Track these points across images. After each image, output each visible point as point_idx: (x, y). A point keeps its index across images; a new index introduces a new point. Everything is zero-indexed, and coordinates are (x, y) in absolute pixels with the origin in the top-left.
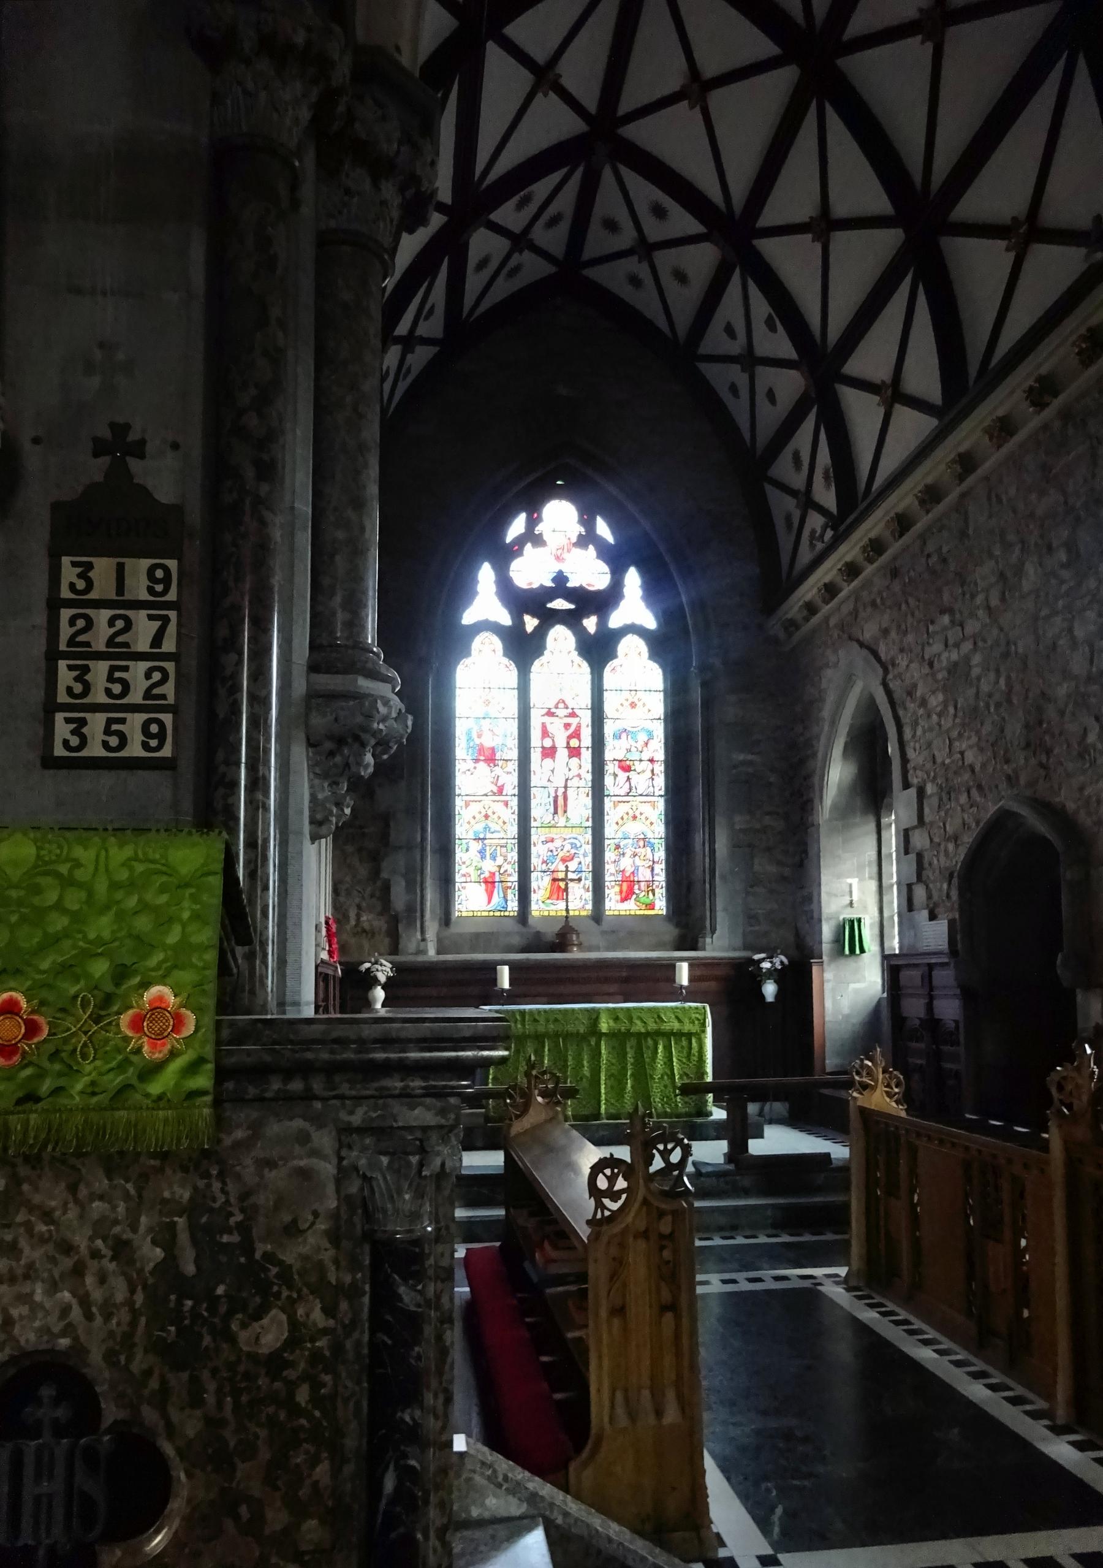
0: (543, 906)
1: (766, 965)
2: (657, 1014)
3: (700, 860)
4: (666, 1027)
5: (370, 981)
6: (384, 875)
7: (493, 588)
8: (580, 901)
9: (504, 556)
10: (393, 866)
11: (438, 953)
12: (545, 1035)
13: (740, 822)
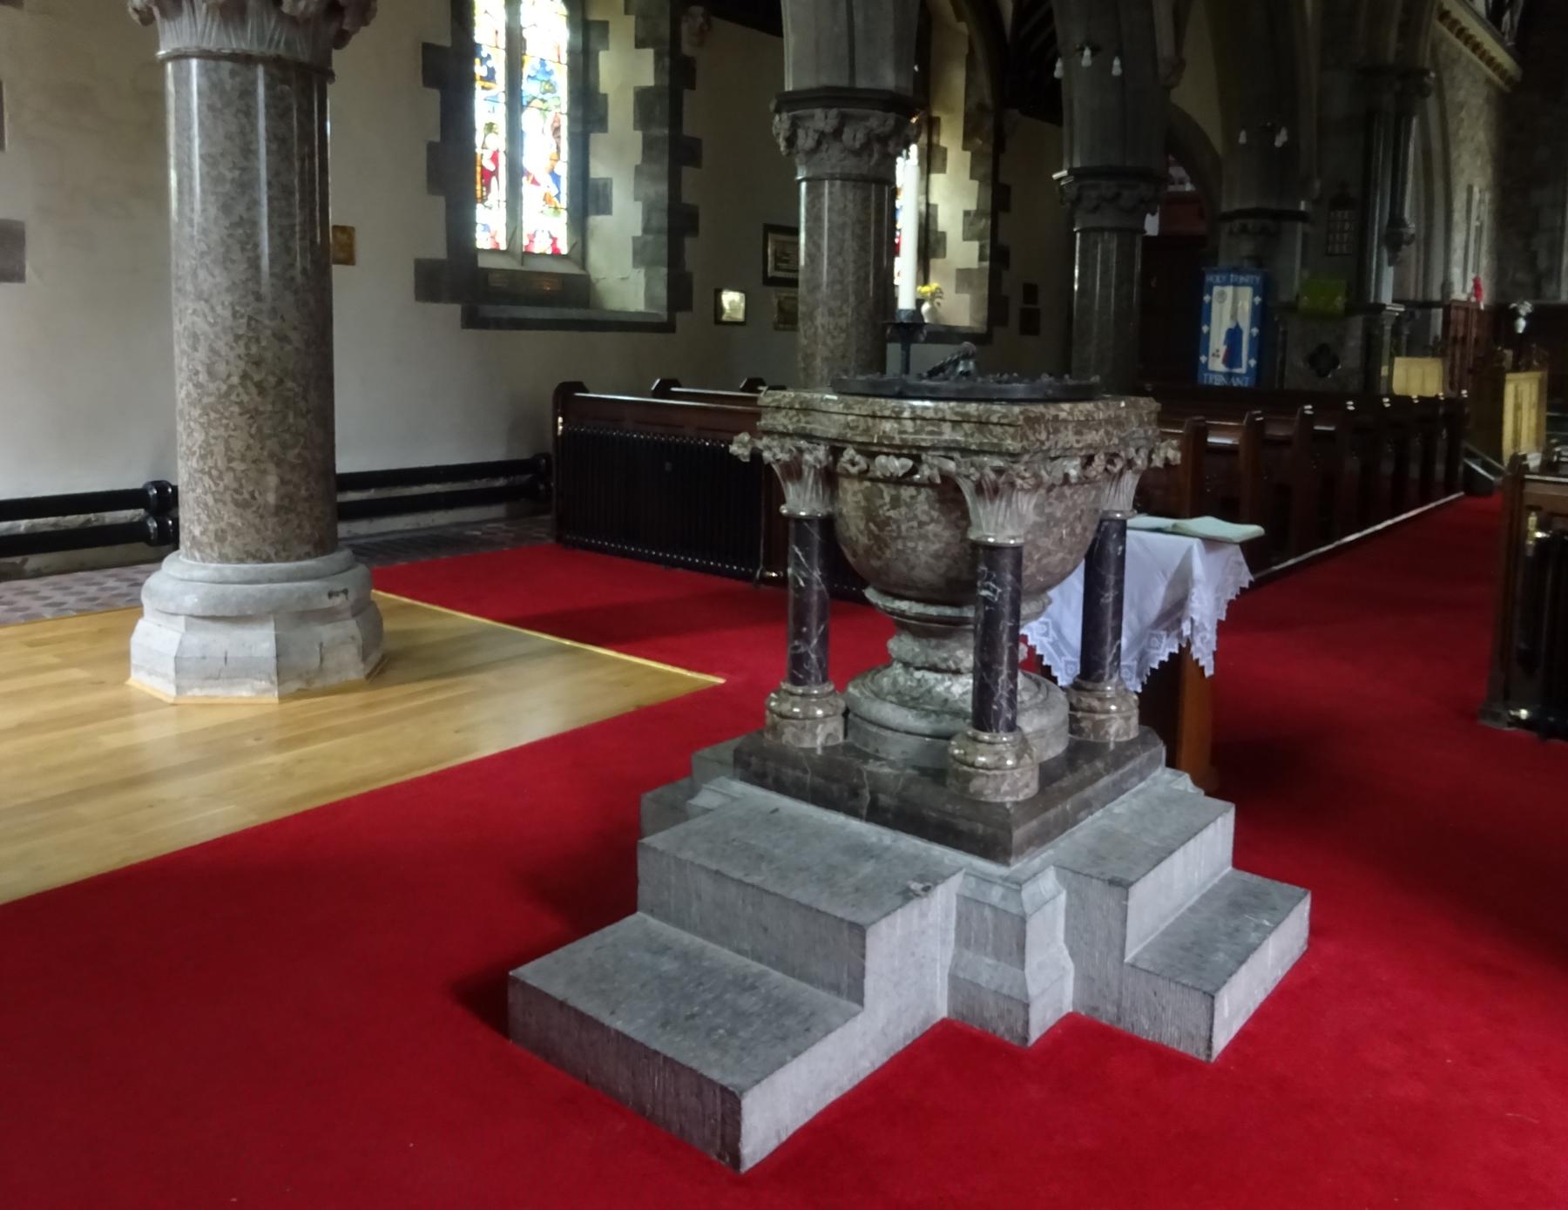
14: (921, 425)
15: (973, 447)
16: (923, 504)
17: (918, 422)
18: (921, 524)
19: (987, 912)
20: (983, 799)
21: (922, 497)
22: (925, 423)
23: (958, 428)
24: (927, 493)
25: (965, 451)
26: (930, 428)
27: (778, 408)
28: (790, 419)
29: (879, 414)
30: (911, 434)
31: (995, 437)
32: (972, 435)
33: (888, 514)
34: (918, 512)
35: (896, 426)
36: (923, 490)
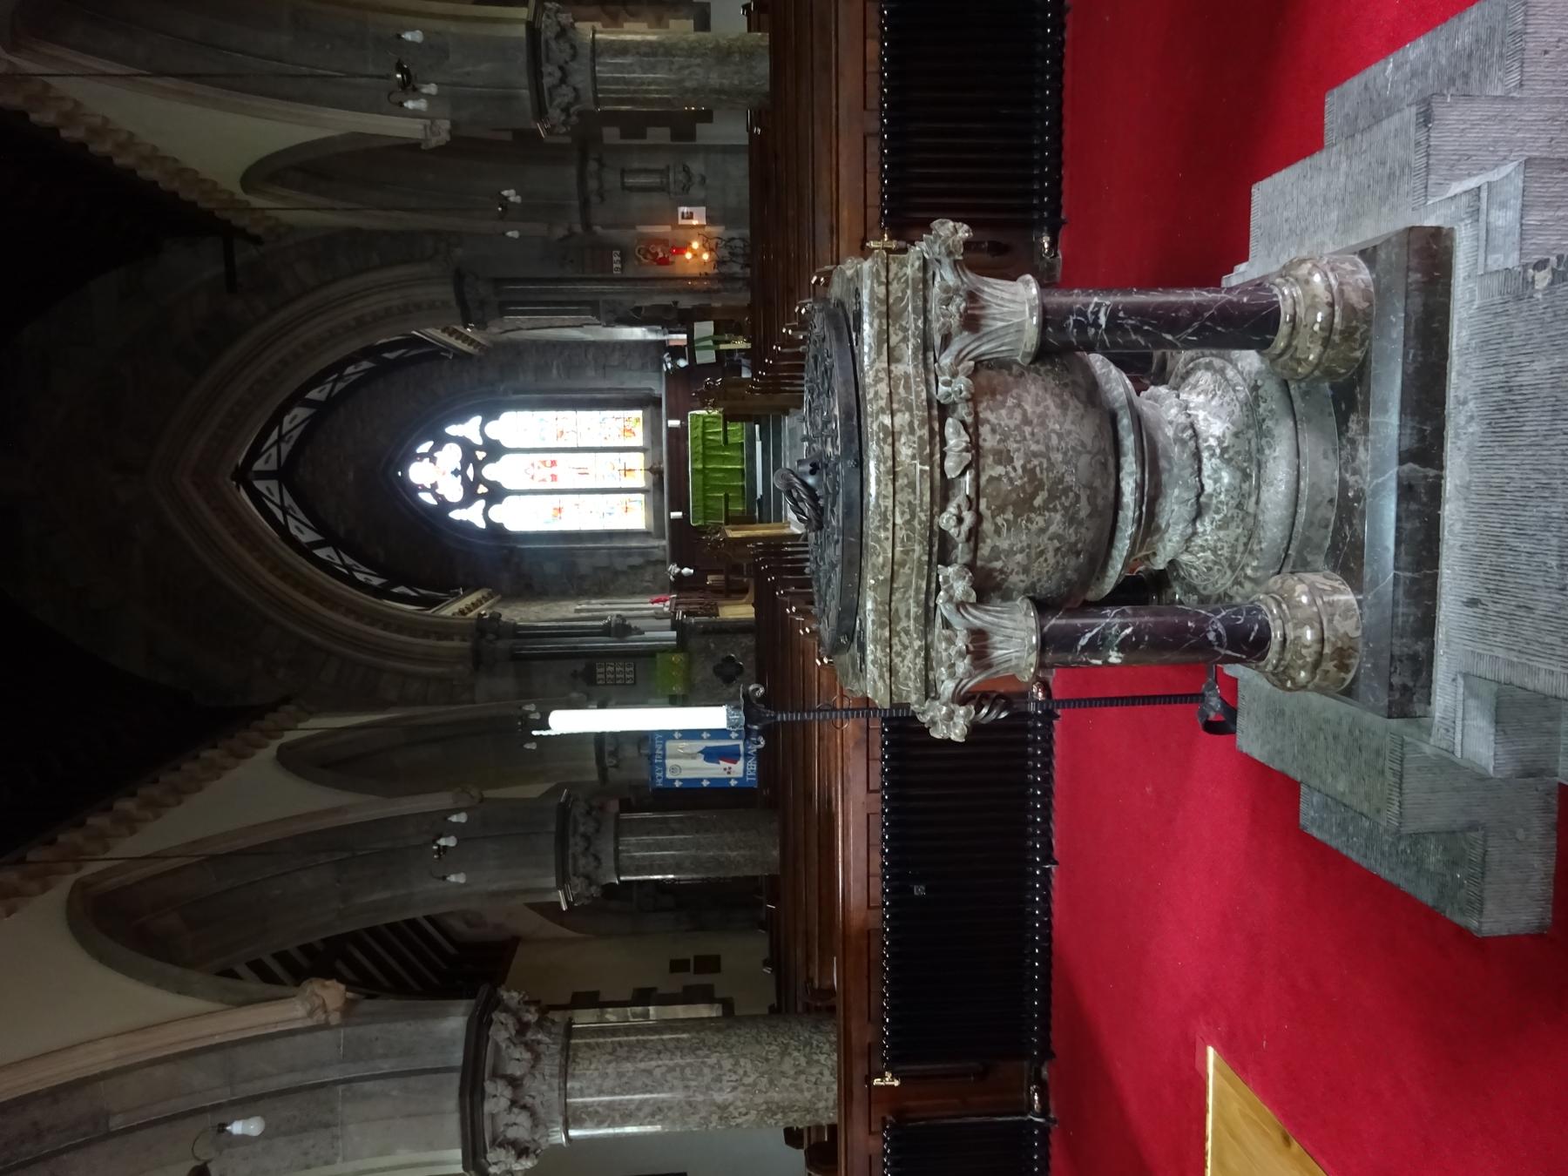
0: (639, 480)
1: (669, 366)
2: (694, 439)
3: (613, 395)
4: (700, 435)
5: (679, 576)
6: (625, 568)
7: (464, 510)
8: (638, 461)
9: (445, 506)
10: (620, 564)
11: (663, 537)
12: (704, 494)
13: (591, 373)
14: (899, 402)
15: (920, 323)
16: (998, 416)
17: (895, 406)
18: (1026, 421)
19: (1533, 219)
20: (1372, 289)
21: (992, 417)
22: (895, 398)
23: (896, 353)
24: (985, 409)
25: (926, 346)
26: (901, 390)
27: (892, 670)
28: (905, 648)
29: (890, 463)
30: (912, 415)
31: (904, 292)
32: (905, 330)
33: (1020, 471)
34: (1012, 423)
35: (903, 440)
36: (981, 416)
